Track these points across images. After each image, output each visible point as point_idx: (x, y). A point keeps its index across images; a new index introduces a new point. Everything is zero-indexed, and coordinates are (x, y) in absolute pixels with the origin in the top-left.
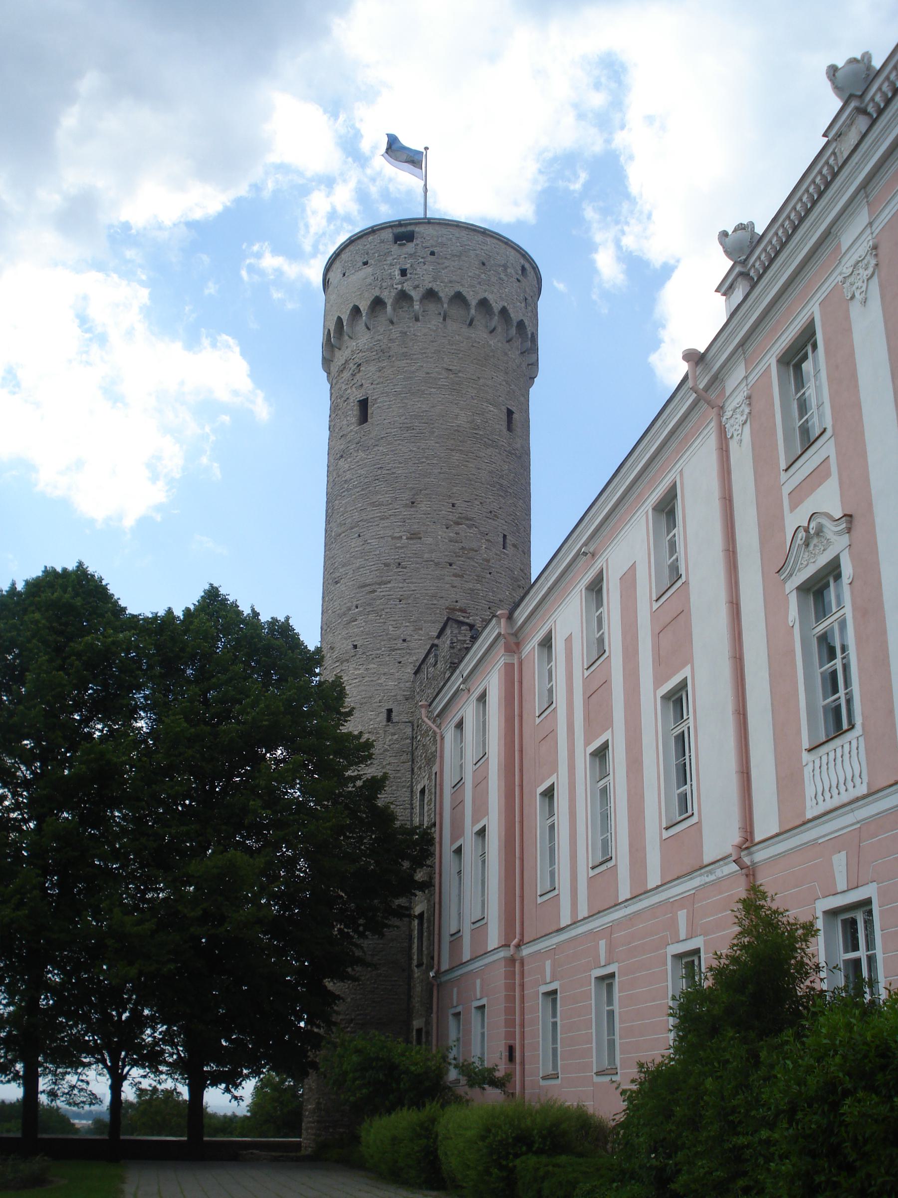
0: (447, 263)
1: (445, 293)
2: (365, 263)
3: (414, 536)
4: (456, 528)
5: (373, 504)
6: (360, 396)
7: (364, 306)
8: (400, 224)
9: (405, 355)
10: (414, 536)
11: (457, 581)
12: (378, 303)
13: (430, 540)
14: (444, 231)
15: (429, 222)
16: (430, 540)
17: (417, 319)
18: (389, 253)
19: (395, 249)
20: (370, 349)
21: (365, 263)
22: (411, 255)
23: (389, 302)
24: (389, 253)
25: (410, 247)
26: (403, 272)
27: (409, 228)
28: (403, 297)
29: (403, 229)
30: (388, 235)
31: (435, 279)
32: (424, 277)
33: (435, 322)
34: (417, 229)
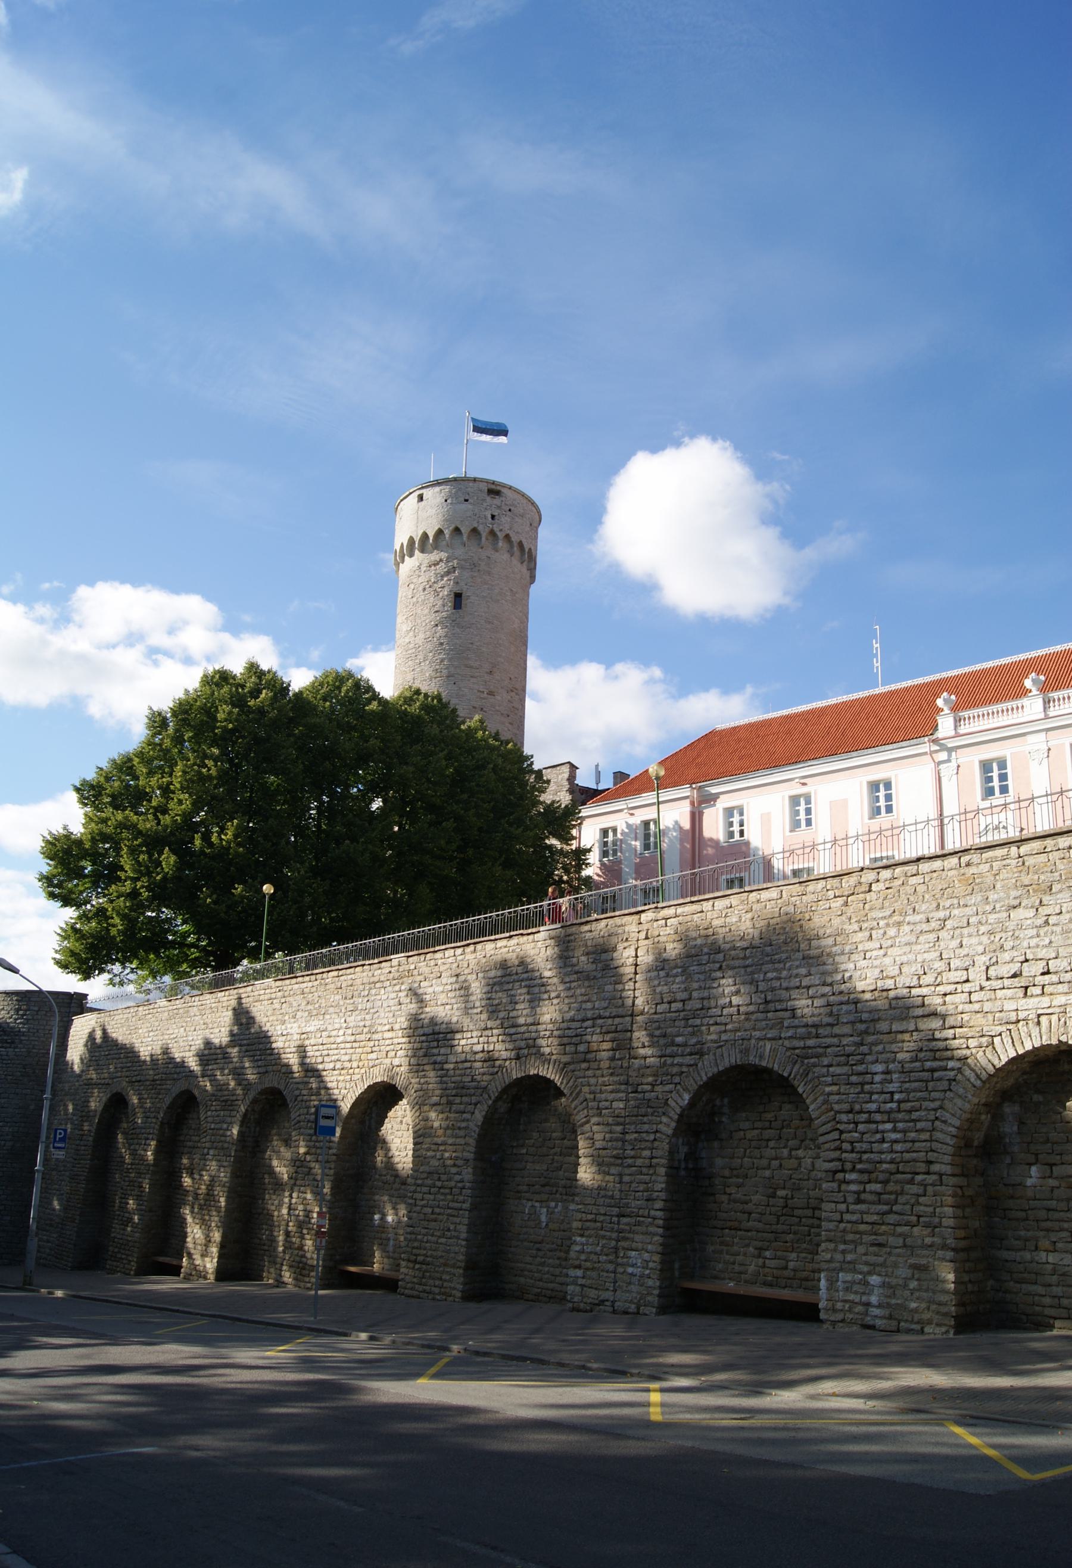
0: (517, 519)
1: (515, 539)
2: (466, 500)
3: (491, 693)
4: (513, 694)
5: (466, 666)
6: (457, 590)
7: (465, 530)
8: (493, 483)
9: (489, 573)
10: (491, 693)
11: (510, 727)
12: (475, 531)
13: (499, 698)
14: (516, 496)
15: (510, 488)
16: (499, 698)
17: (497, 551)
18: (484, 500)
19: (488, 499)
20: (465, 560)
21: (466, 500)
22: (499, 507)
23: (484, 535)
24: (484, 500)
25: (497, 501)
26: (493, 517)
27: (498, 488)
28: (492, 533)
29: (493, 487)
30: (484, 487)
31: (510, 529)
32: (504, 524)
33: (506, 556)
34: (504, 490)
